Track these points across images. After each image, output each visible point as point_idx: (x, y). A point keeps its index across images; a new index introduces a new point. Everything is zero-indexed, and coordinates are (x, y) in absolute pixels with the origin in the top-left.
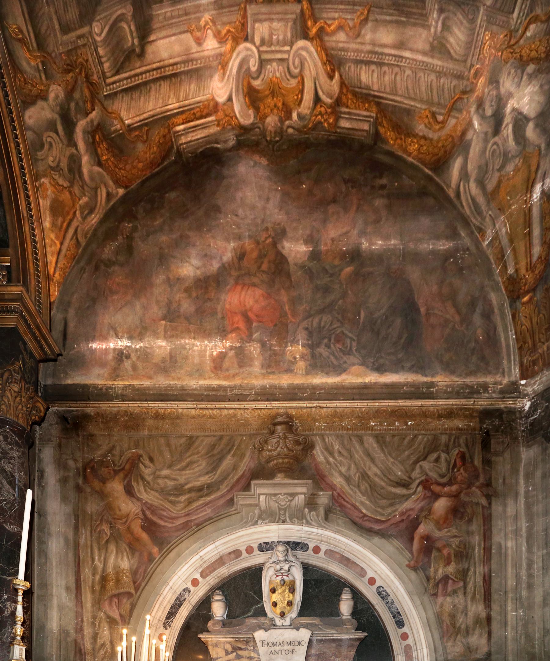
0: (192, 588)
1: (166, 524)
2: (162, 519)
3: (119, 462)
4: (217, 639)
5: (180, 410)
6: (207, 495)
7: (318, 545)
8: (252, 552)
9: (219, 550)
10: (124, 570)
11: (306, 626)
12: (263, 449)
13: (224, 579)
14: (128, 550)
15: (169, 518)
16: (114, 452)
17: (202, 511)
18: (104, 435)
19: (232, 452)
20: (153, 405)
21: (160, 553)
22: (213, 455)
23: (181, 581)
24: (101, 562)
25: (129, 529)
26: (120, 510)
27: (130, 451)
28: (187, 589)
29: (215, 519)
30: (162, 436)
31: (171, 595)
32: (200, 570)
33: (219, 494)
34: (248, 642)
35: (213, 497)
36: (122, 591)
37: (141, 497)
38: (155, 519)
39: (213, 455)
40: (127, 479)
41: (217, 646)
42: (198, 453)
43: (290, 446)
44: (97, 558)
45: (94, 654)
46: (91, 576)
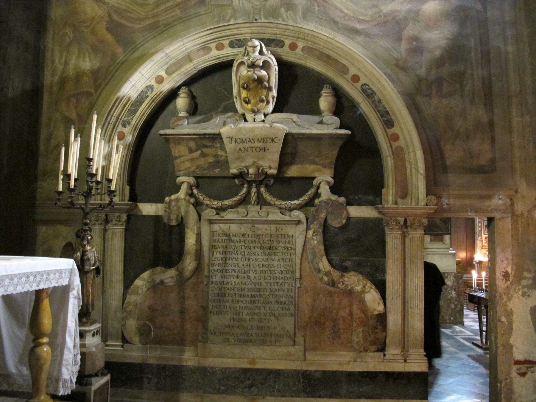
17: (171, 13)
32: (165, 67)
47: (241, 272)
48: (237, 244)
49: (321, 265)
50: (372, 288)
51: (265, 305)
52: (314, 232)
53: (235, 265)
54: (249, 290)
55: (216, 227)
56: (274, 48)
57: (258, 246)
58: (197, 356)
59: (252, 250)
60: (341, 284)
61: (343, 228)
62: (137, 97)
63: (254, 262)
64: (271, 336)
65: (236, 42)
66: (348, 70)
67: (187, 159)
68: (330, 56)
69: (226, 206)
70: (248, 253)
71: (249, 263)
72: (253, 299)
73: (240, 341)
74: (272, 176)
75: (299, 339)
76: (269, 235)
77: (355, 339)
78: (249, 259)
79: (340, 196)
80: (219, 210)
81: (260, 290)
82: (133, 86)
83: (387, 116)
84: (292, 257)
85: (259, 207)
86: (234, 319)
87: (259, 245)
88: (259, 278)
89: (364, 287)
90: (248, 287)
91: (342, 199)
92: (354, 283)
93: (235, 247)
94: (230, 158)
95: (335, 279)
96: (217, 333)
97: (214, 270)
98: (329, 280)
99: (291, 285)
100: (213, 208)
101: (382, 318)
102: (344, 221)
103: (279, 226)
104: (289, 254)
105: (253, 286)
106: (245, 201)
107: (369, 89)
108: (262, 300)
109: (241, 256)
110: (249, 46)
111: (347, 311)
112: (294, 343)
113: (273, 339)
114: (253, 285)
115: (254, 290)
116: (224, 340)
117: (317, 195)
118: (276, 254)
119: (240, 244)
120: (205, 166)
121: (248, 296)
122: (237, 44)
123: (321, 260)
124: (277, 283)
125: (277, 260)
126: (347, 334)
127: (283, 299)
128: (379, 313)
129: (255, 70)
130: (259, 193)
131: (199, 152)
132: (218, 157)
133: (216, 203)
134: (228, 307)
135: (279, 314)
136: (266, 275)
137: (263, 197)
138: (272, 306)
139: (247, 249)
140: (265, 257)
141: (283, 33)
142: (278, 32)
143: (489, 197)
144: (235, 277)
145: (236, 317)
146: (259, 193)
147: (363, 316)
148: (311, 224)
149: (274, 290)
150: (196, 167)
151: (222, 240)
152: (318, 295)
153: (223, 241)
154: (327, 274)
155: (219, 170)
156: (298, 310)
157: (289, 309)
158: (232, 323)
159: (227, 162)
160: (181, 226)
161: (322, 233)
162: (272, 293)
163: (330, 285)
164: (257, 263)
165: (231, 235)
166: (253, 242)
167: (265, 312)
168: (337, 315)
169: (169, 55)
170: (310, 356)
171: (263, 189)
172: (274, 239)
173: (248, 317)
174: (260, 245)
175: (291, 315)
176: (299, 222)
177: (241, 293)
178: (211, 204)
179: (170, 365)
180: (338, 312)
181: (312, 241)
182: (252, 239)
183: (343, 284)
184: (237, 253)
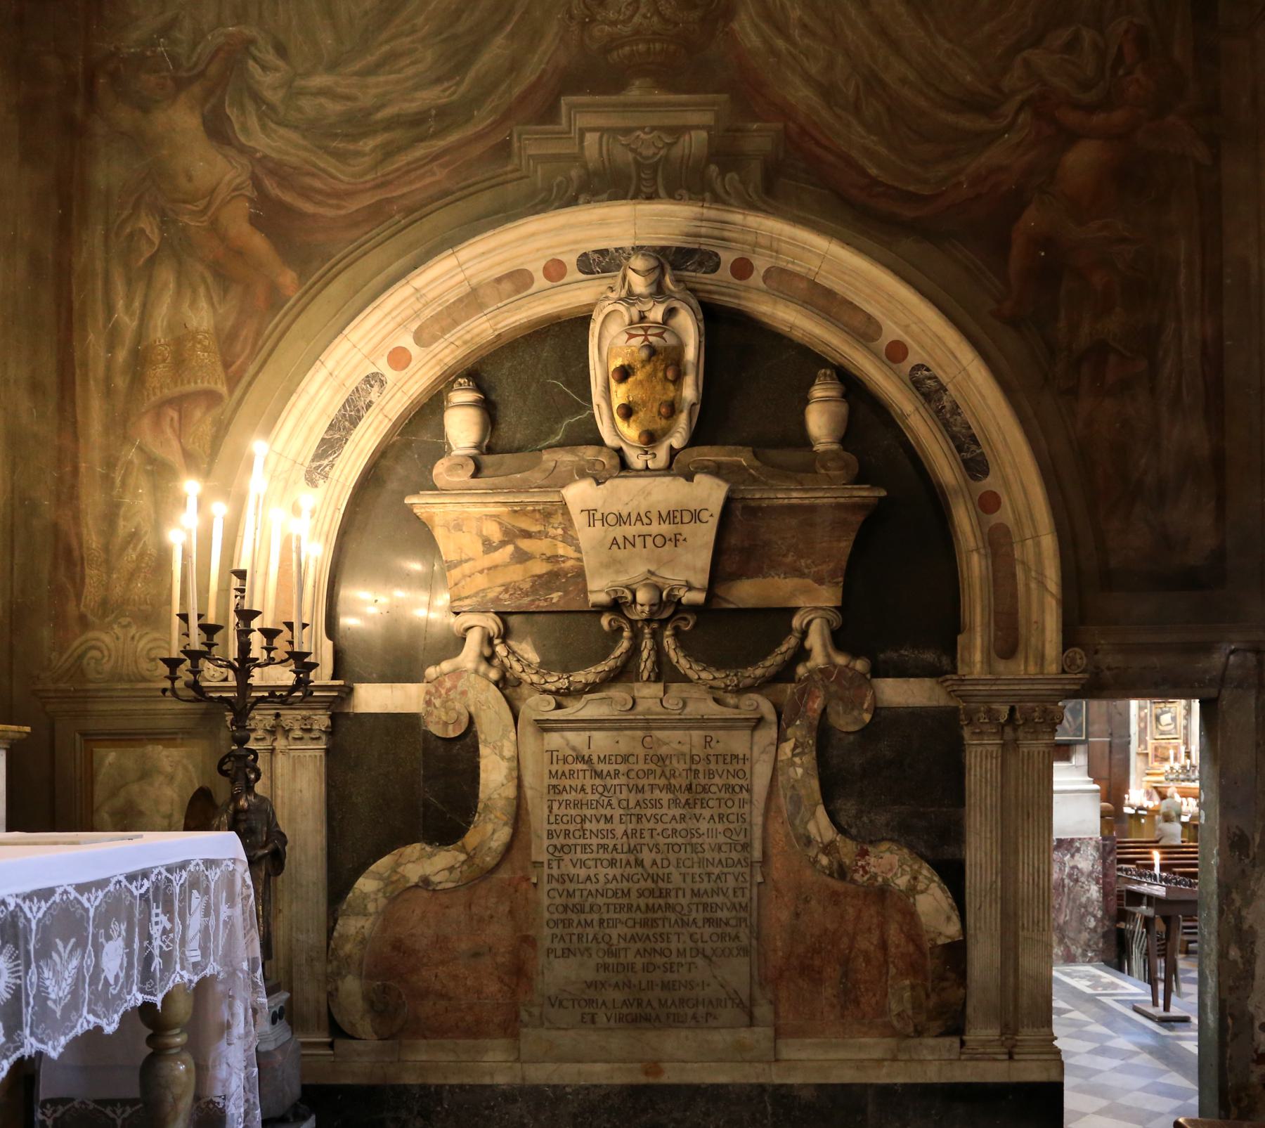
0: (390, 374)
1: (321, 210)
2: (308, 198)
4: (458, 508)
6: (435, 135)
7: (746, 255)
8: (562, 276)
9: (468, 273)
10: (197, 332)
11: (717, 471)
12: (593, 20)
13: (481, 347)
14: (210, 279)
15: (328, 195)
17: (422, 176)
19: (509, 28)
21: (301, 284)
23: (359, 356)
24: (131, 316)
25: (214, 227)
26: (190, 179)
28: (375, 375)
29: (458, 195)
33: (469, 131)
34: (547, 516)
35: (453, 138)
36: (191, 387)
37: (251, 144)
38: (288, 198)
40: (213, 101)
41: (458, 527)
42: (413, 31)
43: (668, 12)
44: (120, 304)
45: (107, 561)
46: (102, 353)
47: (620, 850)
48: (609, 782)
49: (811, 827)
50: (934, 881)
51: (679, 930)
52: (794, 749)
53: (605, 833)
54: (641, 894)
55: (554, 740)
56: (693, 274)
57: (661, 785)
58: (517, 1060)
59: (648, 795)
60: (861, 872)
61: (868, 734)
62: (344, 406)
63: (651, 825)
64: (696, 1005)
65: (596, 256)
66: (879, 328)
67: (480, 568)
68: (836, 294)
69: (579, 686)
70: (638, 803)
71: (639, 827)
72: (650, 915)
73: (620, 1020)
74: (693, 608)
75: (763, 1011)
76: (688, 757)
77: (894, 1007)
78: (639, 818)
79: (855, 655)
80: (562, 696)
81: (668, 892)
82: (331, 374)
83: (974, 447)
84: (742, 811)
85: (660, 686)
86: (606, 967)
87: (662, 782)
88: (665, 862)
89: (915, 878)
90: (637, 886)
91: (860, 665)
92: (891, 870)
93: (605, 787)
94: (589, 563)
95: (847, 861)
96: (565, 1003)
97: (555, 847)
98: (831, 863)
99: (741, 878)
100: (545, 691)
101: (956, 953)
102: (867, 717)
103: (712, 733)
104: (737, 803)
105: (650, 884)
106: (624, 673)
107: (930, 378)
108: (673, 917)
109: (622, 812)
110: (633, 270)
111: (875, 938)
112: (752, 1022)
113: (701, 1010)
114: (649, 881)
115: (652, 892)
116: (583, 1018)
117: (802, 654)
118: (704, 804)
119: (616, 782)
120: (527, 586)
121: (638, 907)
122: (599, 264)
123: (814, 814)
124: (709, 874)
125: (708, 817)
126: (874, 995)
127: (723, 914)
128: (949, 941)
129: (649, 332)
130: (659, 650)
131: (510, 549)
132: (558, 562)
133: (556, 679)
134: (590, 938)
135: (714, 951)
136: (682, 855)
137: (670, 661)
138: (698, 931)
139: (634, 792)
140: (677, 812)
141: (716, 233)
142: (703, 231)
143: (1207, 648)
144: (605, 863)
145: (611, 960)
146: (659, 650)
147: (911, 948)
148: (788, 726)
149: (701, 892)
150: (502, 588)
151: (572, 772)
152: (807, 901)
153: (575, 775)
154: (828, 848)
155: (560, 594)
156: (757, 939)
157: (737, 937)
158: (602, 976)
159: (580, 574)
160: (468, 739)
161: (814, 748)
162: (695, 900)
163: (836, 875)
164: (660, 827)
165: (595, 759)
166: (647, 774)
167: (681, 946)
168: (851, 948)
169: (424, 292)
170: (791, 1050)
171: (669, 642)
172: (700, 767)
173: (639, 962)
174: (666, 782)
175: (745, 951)
176: (759, 722)
177: (620, 901)
178: (543, 681)
179: (452, 1086)
180: (853, 939)
181: (791, 769)
182: (646, 767)
183: (866, 872)
184: (609, 804)
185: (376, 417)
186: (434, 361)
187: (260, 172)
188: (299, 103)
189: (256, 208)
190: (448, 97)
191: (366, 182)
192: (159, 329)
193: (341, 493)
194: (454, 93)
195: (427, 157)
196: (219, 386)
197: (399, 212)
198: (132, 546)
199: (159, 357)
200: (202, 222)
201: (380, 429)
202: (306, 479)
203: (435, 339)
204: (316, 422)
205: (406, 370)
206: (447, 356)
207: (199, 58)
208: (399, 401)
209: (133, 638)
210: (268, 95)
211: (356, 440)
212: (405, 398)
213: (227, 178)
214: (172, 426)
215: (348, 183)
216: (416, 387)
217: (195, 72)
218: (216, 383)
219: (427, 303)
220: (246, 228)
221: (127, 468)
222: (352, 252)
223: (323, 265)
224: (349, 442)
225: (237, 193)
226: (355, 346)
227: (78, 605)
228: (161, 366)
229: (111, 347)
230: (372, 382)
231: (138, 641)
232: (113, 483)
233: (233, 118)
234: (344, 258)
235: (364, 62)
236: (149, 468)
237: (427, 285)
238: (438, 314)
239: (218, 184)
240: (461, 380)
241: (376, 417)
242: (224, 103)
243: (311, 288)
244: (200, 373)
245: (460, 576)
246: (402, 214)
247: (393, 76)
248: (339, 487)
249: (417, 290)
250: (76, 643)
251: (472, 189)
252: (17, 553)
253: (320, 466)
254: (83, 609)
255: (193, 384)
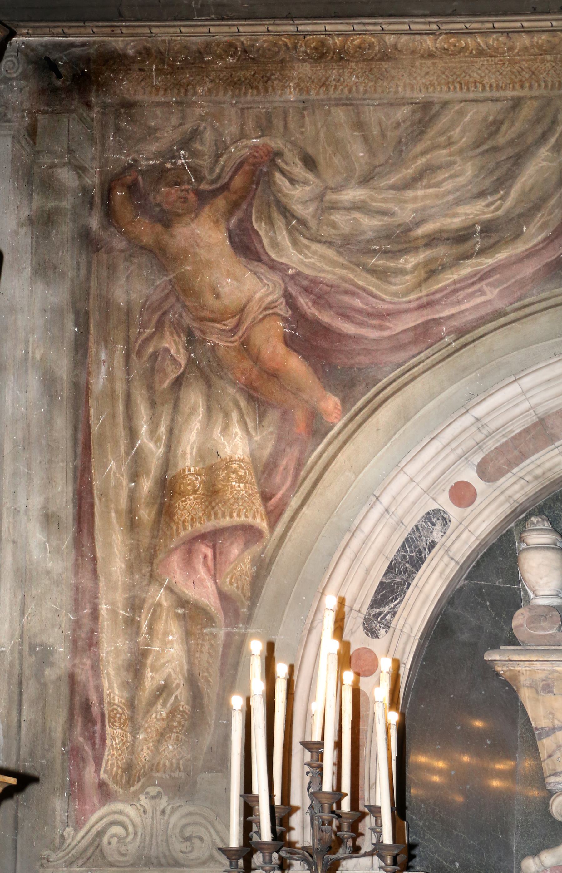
1: (363, 331)
2: (347, 318)
3: (212, 170)
4: (548, 667)
5: (390, 40)
6: (482, 252)
9: (534, 401)
10: (231, 460)
14: (243, 403)
15: (369, 315)
16: (198, 146)
18: (167, 104)
19: (553, 140)
20: (309, 28)
21: (345, 410)
22: (495, 149)
24: (157, 441)
26: (218, 296)
27: (245, 142)
28: (436, 512)
29: (512, 316)
30: (339, 103)
31: (386, 532)
32: (477, 459)
33: (520, 247)
35: (502, 255)
36: (226, 522)
37: (283, 260)
38: (326, 318)
39: (495, 149)
40: (239, 214)
41: (548, 688)
42: (450, 143)
44: (144, 429)
45: (131, 719)
46: (124, 481)
62: (403, 546)
82: (387, 510)
169: (485, 421)
185: (441, 559)
186: (502, 498)
187: (293, 290)
188: (332, 217)
189: (292, 329)
190: (494, 211)
191: (410, 302)
192: (188, 456)
193: (406, 644)
194: (497, 209)
195: (475, 275)
196: (258, 520)
197: (448, 334)
198: (80, 468)
199: (189, 488)
200: (233, 342)
201: (447, 573)
202: (365, 628)
203: (501, 473)
204: (373, 564)
205: (471, 508)
206: (517, 492)
207: (222, 170)
208: (466, 542)
209: (163, 812)
210: (298, 209)
211: (420, 584)
212: (473, 538)
213: (258, 295)
214: (205, 563)
215: (391, 303)
216: (484, 525)
217: (218, 185)
218: (254, 517)
219: (490, 434)
220: (281, 349)
221: (155, 611)
222: (399, 377)
223: (369, 390)
224: (411, 588)
225: (271, 311)
226: (412, 480)
227: (97, 771)
228: (191, 497)
229: (135, 476)
230: (434, 520)
231: (170, 816)
232: (139, 627)
233: (262, 233)
234: (391, 383)
235: (399, 176)
236: (180, 611)
237: (488, 414)
238: (502, 445)
239: (248, 302)
240: (534, 519)
241: (441, 559)
242: (251, 216)
243: (356, 414)
244: (235, 506)
245: (554, 746)
246: (453, 336)
247: (431, 191)
248: (404, 638)
249: (478, 420)
250: (93, 819)
251: (527, 310)
252: (25, 707)
253: (380, 614)
254: (103, 775)
255: (228, 518)
